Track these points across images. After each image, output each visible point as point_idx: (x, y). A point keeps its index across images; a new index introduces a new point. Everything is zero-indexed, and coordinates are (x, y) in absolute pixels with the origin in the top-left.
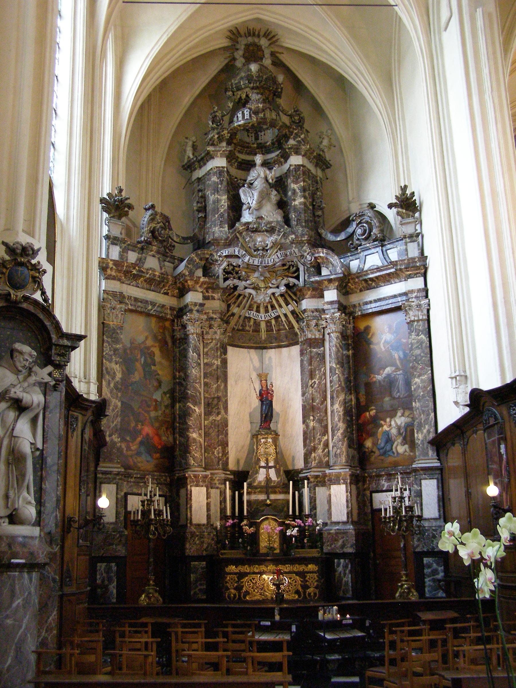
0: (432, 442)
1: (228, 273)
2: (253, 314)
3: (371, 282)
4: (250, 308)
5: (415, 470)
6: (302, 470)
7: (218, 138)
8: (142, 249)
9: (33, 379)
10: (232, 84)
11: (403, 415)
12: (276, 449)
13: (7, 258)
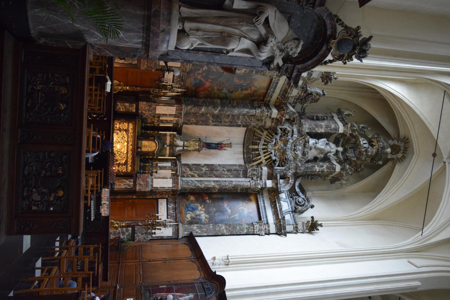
0: (191, 233)
1: (284, 131)
2: (262, 142)
3: (274, 204)
6: (180, 162)
7: (354, 129)
8: (303, 88)
9: (277, 53)
10: (381, 138)
11: (206, 218)
12: (193, 150)
13: (360, 39)
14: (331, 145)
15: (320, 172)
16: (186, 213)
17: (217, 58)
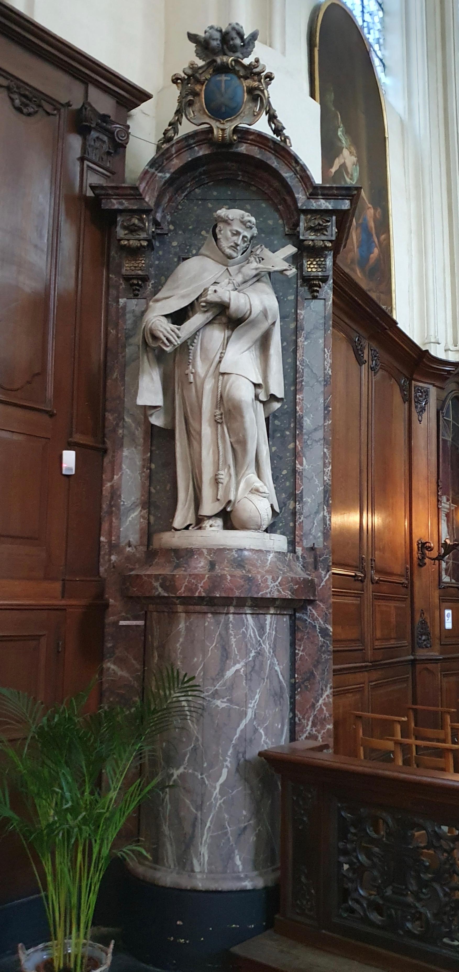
13: (200, 63)
17: (308, 421)
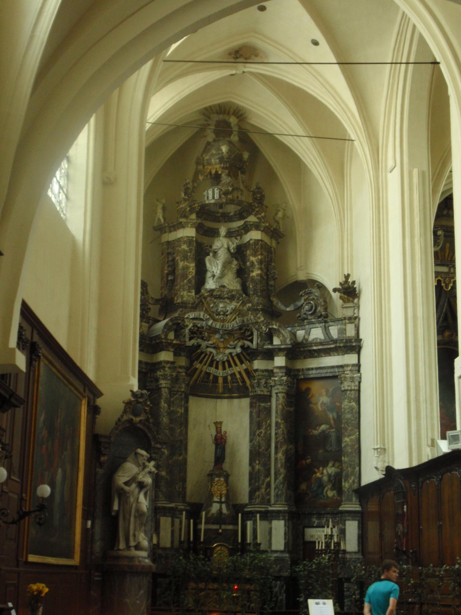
2: (212, 370)
4: (211, 365)
5: (342, 512)
9: (147, 470)
12: (227, 486)
13: (133, 399)
14: (216, 248)
15: (263, 266)
16: (326, 498)
